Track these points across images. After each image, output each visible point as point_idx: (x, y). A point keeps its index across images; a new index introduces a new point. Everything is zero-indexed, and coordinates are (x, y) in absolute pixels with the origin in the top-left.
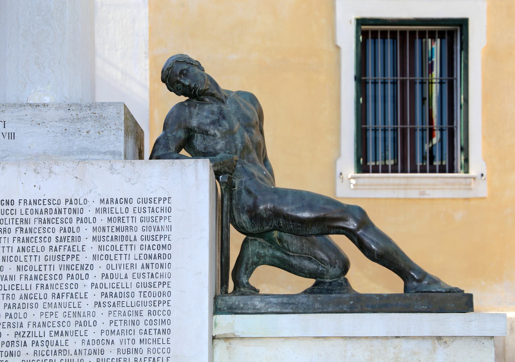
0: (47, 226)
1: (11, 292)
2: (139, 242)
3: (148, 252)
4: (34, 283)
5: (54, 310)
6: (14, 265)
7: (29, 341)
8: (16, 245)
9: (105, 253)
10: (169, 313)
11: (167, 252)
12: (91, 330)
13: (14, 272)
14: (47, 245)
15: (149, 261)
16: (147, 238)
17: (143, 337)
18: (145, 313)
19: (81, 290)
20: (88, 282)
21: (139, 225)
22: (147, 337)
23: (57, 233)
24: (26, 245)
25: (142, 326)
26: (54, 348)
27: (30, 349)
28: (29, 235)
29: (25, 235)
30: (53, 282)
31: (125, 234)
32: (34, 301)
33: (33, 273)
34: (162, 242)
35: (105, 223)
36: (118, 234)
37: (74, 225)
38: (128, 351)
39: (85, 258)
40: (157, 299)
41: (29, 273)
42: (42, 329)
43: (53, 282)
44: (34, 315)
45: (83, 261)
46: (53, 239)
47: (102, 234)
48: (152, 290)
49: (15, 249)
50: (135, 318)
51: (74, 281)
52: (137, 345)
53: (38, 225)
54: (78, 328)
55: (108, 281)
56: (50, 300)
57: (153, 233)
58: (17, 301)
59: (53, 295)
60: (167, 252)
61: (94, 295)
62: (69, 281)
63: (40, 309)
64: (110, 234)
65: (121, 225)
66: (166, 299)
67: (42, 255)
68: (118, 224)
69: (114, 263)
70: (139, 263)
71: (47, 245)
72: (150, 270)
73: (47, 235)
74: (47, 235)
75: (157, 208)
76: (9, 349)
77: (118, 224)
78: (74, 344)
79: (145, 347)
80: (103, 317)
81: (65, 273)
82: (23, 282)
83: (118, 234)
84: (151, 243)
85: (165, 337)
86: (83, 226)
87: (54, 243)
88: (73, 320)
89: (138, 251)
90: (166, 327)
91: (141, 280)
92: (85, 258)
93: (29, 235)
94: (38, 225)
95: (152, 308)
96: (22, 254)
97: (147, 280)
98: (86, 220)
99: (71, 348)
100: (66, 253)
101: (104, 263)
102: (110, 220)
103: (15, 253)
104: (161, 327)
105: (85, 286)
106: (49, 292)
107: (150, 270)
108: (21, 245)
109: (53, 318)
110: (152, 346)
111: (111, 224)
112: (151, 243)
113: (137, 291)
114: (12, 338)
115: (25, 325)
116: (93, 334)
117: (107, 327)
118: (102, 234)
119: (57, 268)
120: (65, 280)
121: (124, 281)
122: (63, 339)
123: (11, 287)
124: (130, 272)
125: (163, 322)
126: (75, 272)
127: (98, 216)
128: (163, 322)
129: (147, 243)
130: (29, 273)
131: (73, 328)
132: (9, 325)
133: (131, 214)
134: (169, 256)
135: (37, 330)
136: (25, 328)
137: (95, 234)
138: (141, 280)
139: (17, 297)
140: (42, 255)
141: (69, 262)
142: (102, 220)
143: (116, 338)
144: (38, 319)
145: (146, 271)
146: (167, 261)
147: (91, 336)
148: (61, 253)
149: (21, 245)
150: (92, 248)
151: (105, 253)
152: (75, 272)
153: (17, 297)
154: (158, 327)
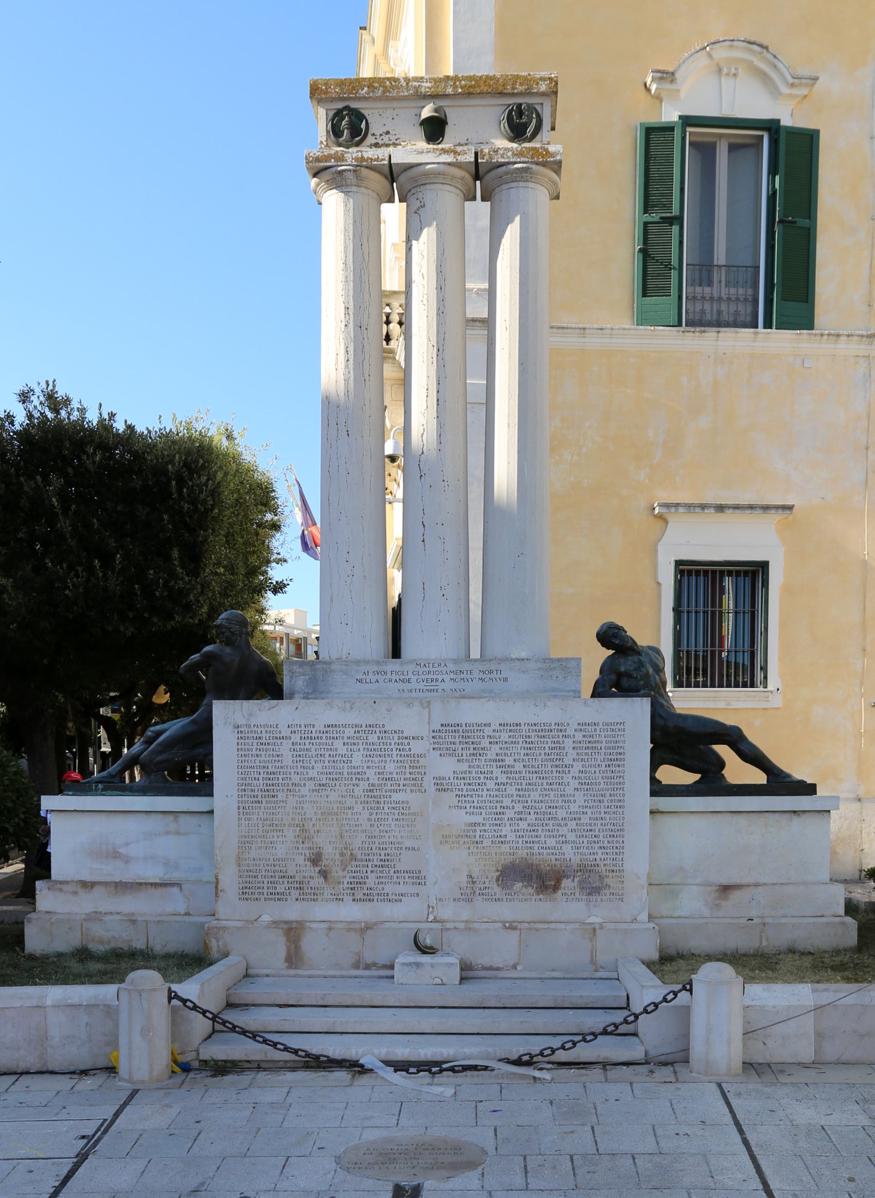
0: (542, 740)
1: (520, 781)
2: (603, 750)
3: (610, 757)
4: (535, 775)
5: (548, 793)
6: (521, 764)
7: (532, 812)
8: (523, 752)
9: (581, 757)
10: (624, 795)
11: (622, 757)
12: (572, 805)
13: (521, 768)
14: (543, 752)
15: (610, 763)
16: (609, 748)
17: (606, 810)
18: (608, 795)
19: (565, 780)
20: (570, 776)
21: (604, 740)
22: (609, 810)
23: (549, 744)
24: (529, 752)
25: (606, 803)
26: (548, 816)
27: (533, 817)
28: (531, 746)
29: (529, 746)
30: (547, 775)
31: (594, 745)
32: (535, 787)
33: (534, 770)
34: (619, 751)
35: (581, 739)
36: (590, 745)
37: (561, 739)
38: (597, 819)
39: (567, 761)
40: (616, 786)
41: (531, 769)
42: (540, 805)
43: (547, 775)
44: (535, 795)
45: (566, 762)
46: (547, 748)
47: (579, 745)
48: (612, 781)
49: (522, 754)
50: (601, 798)
51: (561, 775)
52: (603, 815)
53: (537, 739)
54: (563, 804)
55: (583, 775)
56: (545, 786)
57: (612, 745)
58: (524, 787)
59: (547, 784)
60: (622, 757)
61: (574, 784)
62: (558, 775)
63: (539, 792)
64: (584, 745)
65: (592, 739)
66: (622, 786)
67: (540, 758)
68: (589, 739)
69: (587, 764)
70: (604, 764)
71: (543, 752)
72: (611, 769)
73: (543, 745)
74: (543, 745)
75: (616, 728)
76: (519, 816)
77: (589, 739)
78: (561, 814)
79: (608, 816)
80: (580, 797)
81: (554, 770)
82: (528, 775)
83: (590, 745)
84: (612, 751)
85: (621, 810)
86: (566, 740)
87: (547, 751)
88: (560, 799)
89: (603, 756)
90: (621, 804)
91: (605, 774)
92: (567, 761)
93: (531, 746)
94: (537, 739)
95: (612, 793)
96: (526, 758)
97: (609, 775)
98: (569, 736)
99: (560, 816)
100: (556, 757)
101: (581, 763)
102: (584, 736)
103: (522, 757)
104: (618, 804)
105: (567, 778)
106: (545, 782)
107: (611, 769)
108: (526, 752)
109: (547, 798)
110: (612, 816)
111: (585, 739)
112: (612, 751)
113: (602, 782)
114: (521, 809)
115: (529, 802)
116: (573, 808)
117: (582, 803)
118: (579, 745)
119: (549, 766)
120: (554, 774)
121: (594, 775)
122: (554, 810)
123: (520, 778)
124: (597, 770)
125: (620, 801)
126: (561, 769)
127: (577, 734)
128: (620, 801)
129: (609, 751)
130: (531, 769)
131: (560, 804)
132: (519, 801)
133: (598, 732)
134: (624, 760)
135: (537, 805)
136: (529, 804)
137: (574, 745)
138: (605, 774)
139: (524, 784)
140: (540, 758)
141: (557, 763)
142: (579, 736)
143: (589, 811)
144: (537, 799)
145: (608, 769)
146: (622, 763)
147: (572, 809)
148: (552, 757)
149: (526, 752)
150: (572, 754)
151: (581, 757)
152: (561, 769)
153: (524, 784)
154: (616, 804)
